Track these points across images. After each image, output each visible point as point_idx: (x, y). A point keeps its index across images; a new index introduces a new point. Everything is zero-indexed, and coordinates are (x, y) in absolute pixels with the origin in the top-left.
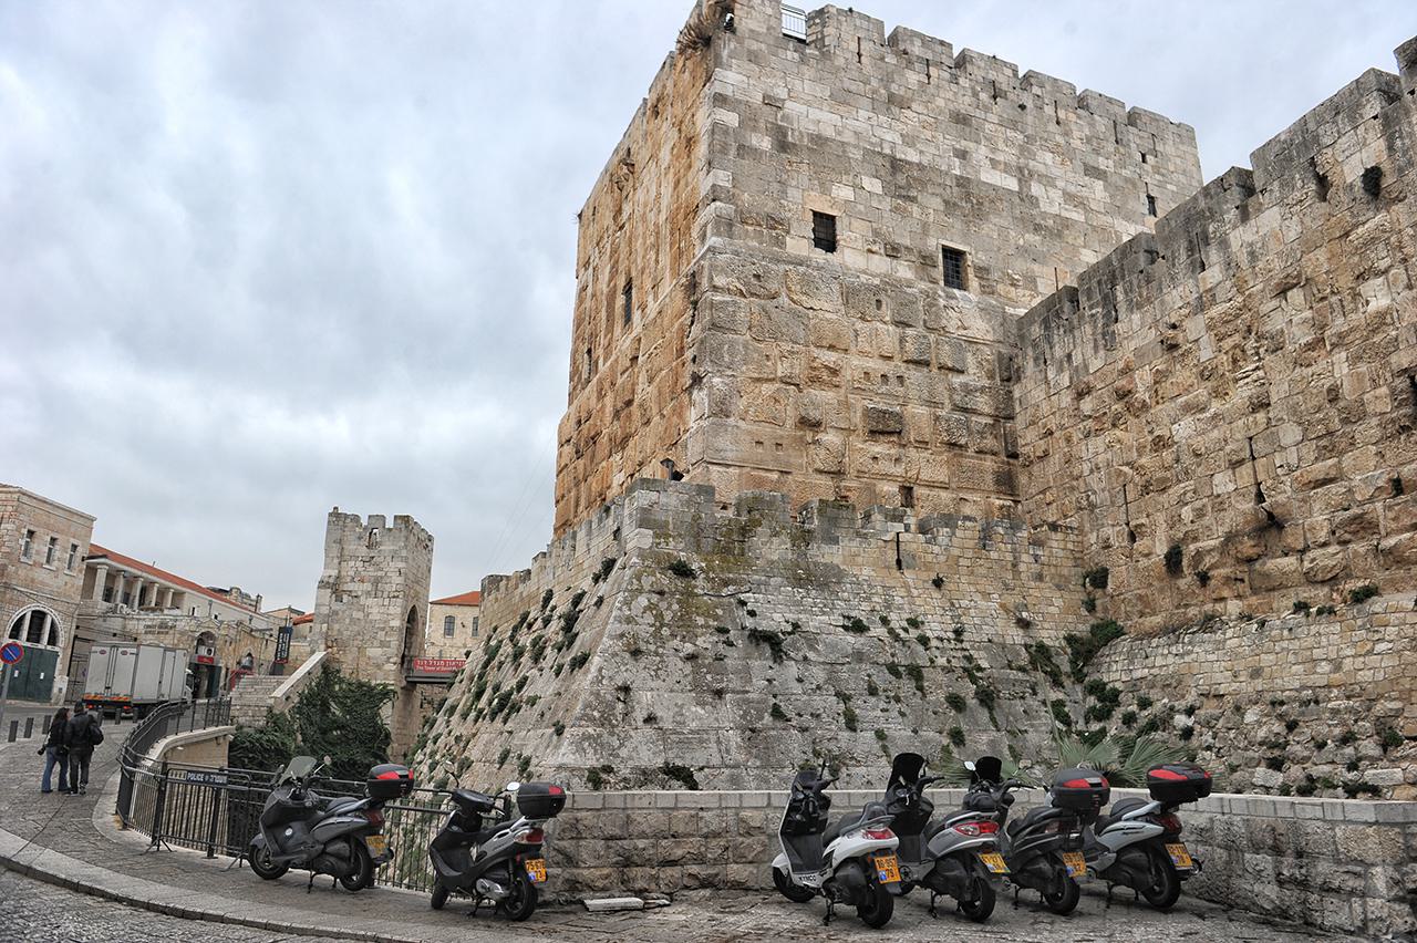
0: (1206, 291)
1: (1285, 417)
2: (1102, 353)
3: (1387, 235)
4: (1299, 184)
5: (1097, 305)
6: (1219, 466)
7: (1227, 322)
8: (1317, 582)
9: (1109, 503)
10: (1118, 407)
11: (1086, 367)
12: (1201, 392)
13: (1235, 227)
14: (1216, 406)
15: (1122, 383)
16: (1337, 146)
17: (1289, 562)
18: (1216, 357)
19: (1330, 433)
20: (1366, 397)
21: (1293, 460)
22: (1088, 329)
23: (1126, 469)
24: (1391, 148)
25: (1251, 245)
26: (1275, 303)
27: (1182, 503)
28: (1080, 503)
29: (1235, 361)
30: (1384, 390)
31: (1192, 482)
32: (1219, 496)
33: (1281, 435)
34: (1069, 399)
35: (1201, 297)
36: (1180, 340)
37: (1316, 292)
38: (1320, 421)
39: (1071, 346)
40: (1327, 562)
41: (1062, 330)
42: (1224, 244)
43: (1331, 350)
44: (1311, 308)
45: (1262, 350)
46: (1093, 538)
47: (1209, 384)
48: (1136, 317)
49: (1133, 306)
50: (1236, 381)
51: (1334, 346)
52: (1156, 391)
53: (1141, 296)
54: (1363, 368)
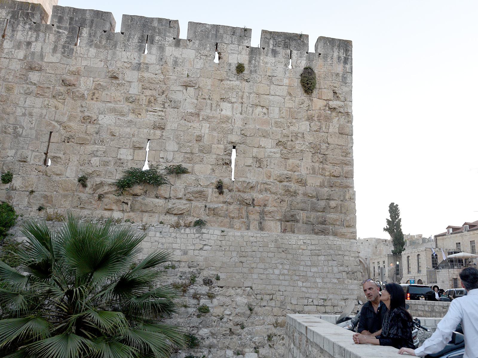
0: (144, 63)
1: (172, 138)
2: (59, 55)
3: (239, 90)
5: (65, 29)
6: (125, 146)
7: (151, 83)
8: (172, 214)
9: (34, 137)
10: (62, 89)
11: (42, 57)
12: (125, 107)
13: (170, 45)
14: (131, 117)
15: (71, 78)
16: (229, 46)
17: (160, 202)
18: (139, 95)
19: (192, 153)
20: (213, 145)
21: (170, 158)
22: (52, 38)
23: (56, 124)
24: (250, 62)
25: (177, 58)
27: (93, 154)
28: (5, 128)
29: (150, 102)
30: (222, 146)
31: (104, 147)
32: (120, 159)
33: (167, 145)
34: (18, 67)
35: (140, 64)
36: (120, 76)
37: (200, 94)
38: (189, 146)
39: (33, 39)
40: (180, 206)
41: (27, 26)
42: (162, 48)
43: (202, 121)
45: (166, 105)
46: (11, 153)
47: (131, 105)
48: (93, 51)
49: (91, 43)
50: (147, 111)
51: (203, 119)
52: (94, 94)
53: (100, 42)
54: (215, 134)
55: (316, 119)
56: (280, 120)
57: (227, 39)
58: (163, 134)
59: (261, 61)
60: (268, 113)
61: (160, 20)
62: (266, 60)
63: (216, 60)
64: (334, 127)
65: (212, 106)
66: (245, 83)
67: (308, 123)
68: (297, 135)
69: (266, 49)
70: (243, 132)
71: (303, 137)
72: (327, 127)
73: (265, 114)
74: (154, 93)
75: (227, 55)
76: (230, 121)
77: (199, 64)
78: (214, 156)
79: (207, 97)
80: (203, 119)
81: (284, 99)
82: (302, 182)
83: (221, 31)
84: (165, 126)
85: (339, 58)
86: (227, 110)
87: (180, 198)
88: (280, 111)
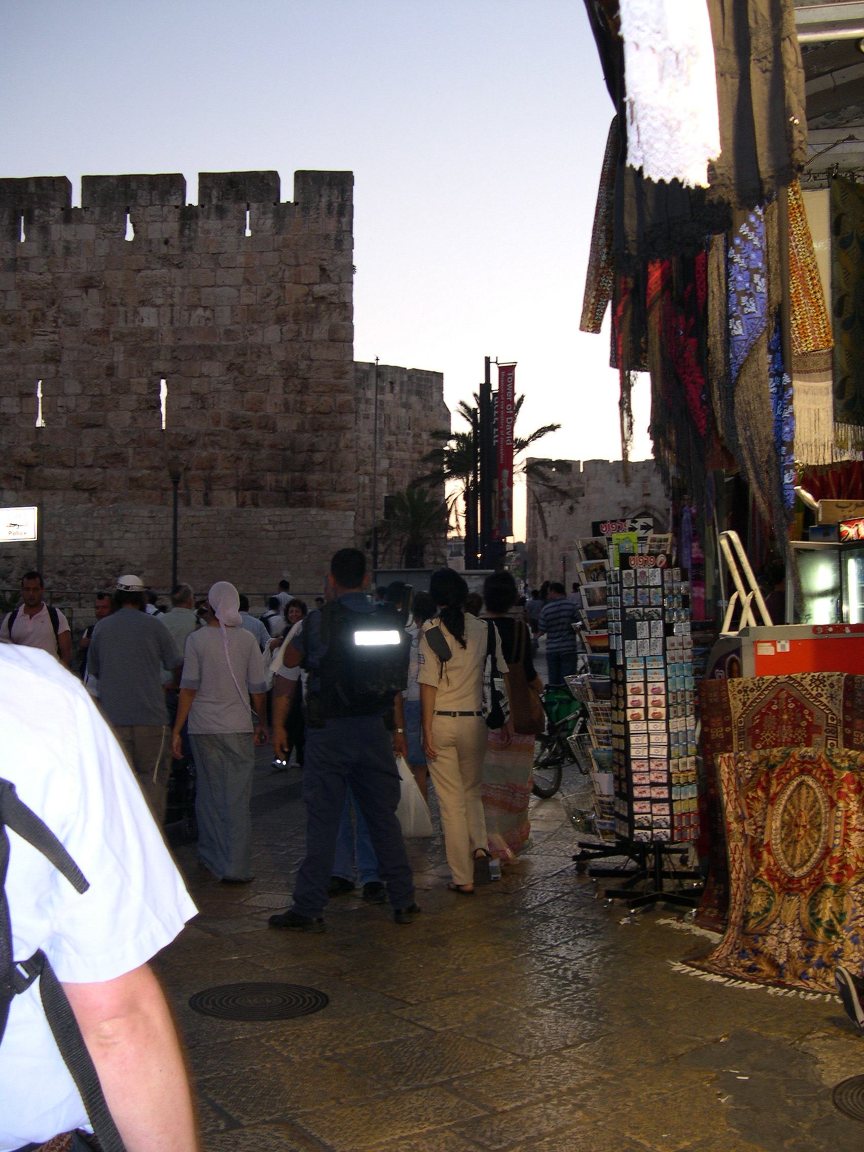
1: (71, 374)
4: (115, 219)
13: (57, 222)
14: (12, 347)
19: (102, 395)
25: (68, 242)
26: (77, 292)
29: (35, 320)
30: (144, 380)
35: (15, 260)
37: (108, 296)
42: (45, 229)
44: (104, 307)
45: (60, 321)
50: (34, 334)
51: (115, 339)
55: (290, 319)
56: (232, 328)
57: (143, 197)
58: (60, 369)
59: (199, 229)
60: (214, 316)
61: (39, 181)
62: (207, 227)
63: (130, 236)
64: (320, 332)
65: (126, 316)
66: (175, 271)
67: (278, 327)
68: (259, 351)
69: (206, 207)
70: (175, 354)
71: (270, 353)
72: (310, 332)
73: (208, 319)
74: (40, 304)
75: (145, 225)
76: (155, 338)
77: (103, 248)
78: (134, 397)
79: (119, 301)
80: (115, 339)
81: (239, 290)
82: (268, 426)
83: (134, 185)
84: (60, 356)
85: (330, 205)
86: (149, 318)
87: (91, 466)
88: (233, 311)
